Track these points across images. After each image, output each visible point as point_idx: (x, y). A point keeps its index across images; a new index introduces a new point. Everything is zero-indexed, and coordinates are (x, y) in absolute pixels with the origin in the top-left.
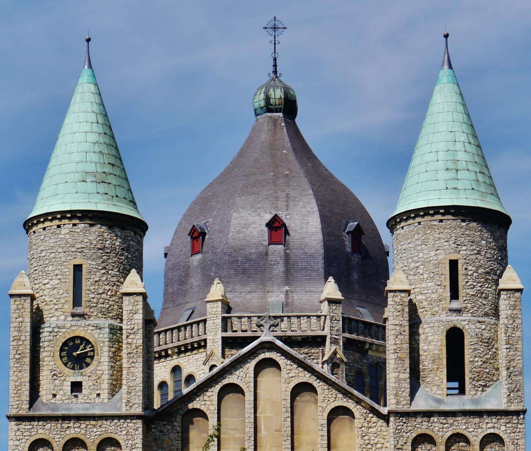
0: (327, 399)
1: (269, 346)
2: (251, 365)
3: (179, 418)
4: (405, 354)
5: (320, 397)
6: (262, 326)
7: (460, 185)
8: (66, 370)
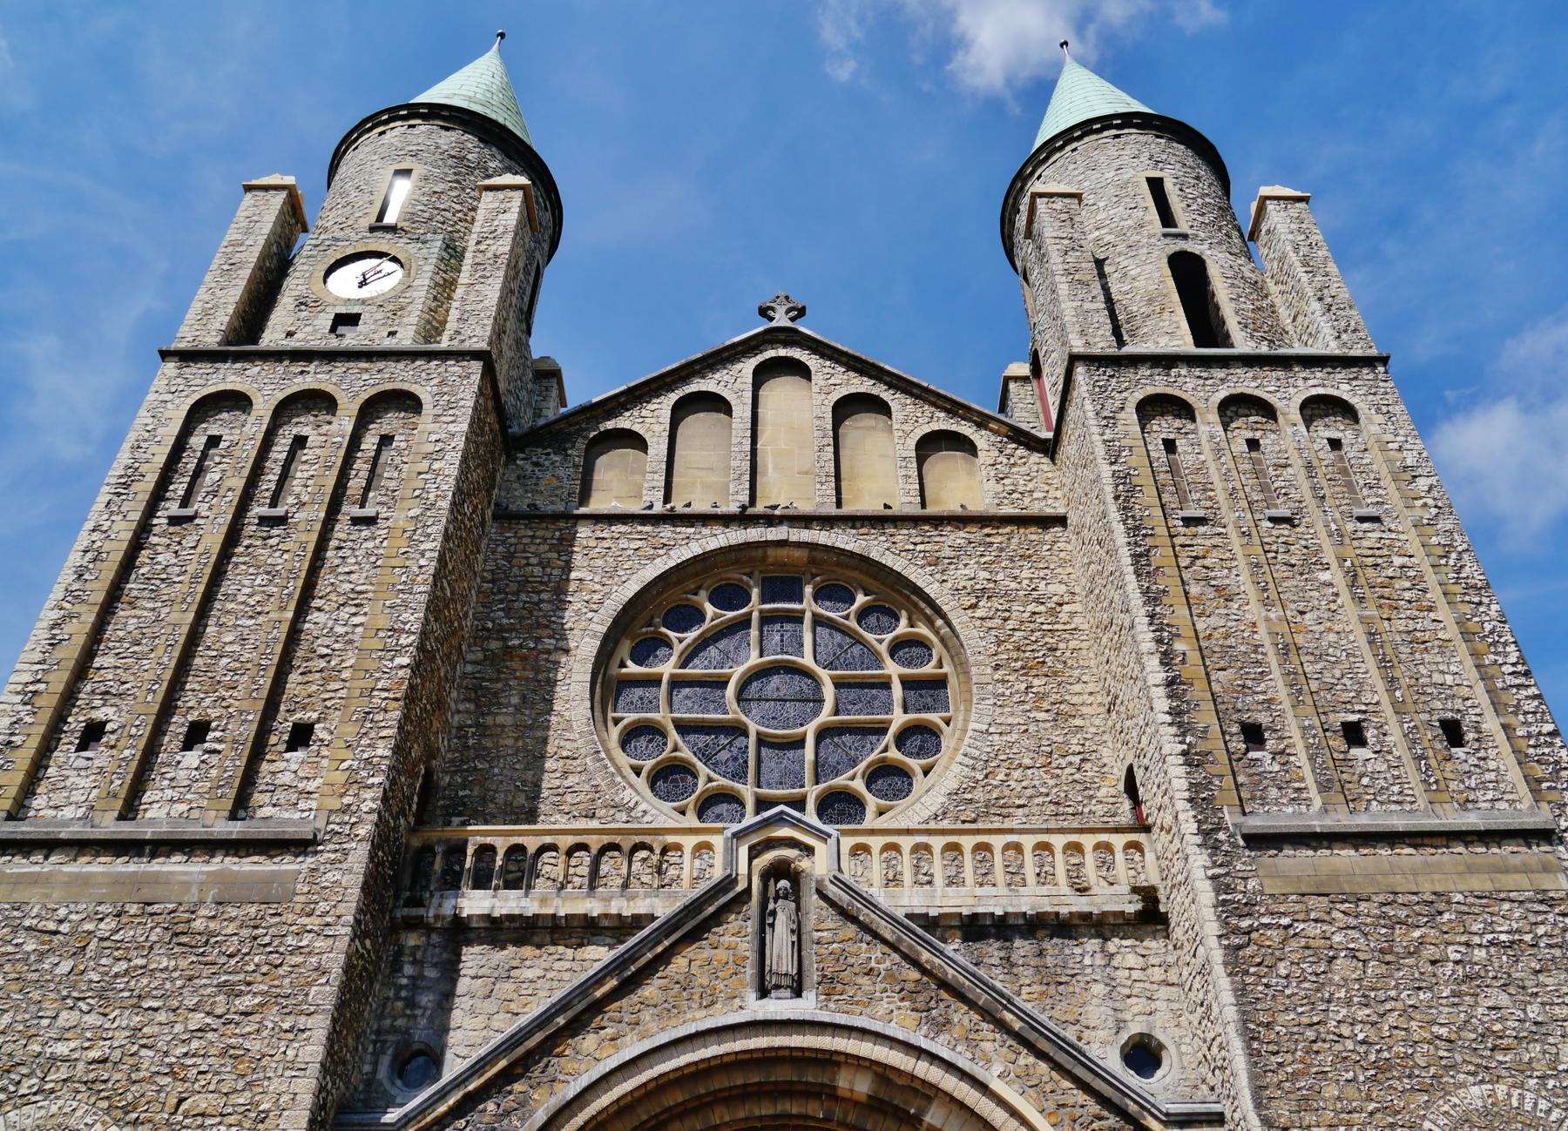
2: (748, 366)
3: (581, 444)
6: (773, 309)
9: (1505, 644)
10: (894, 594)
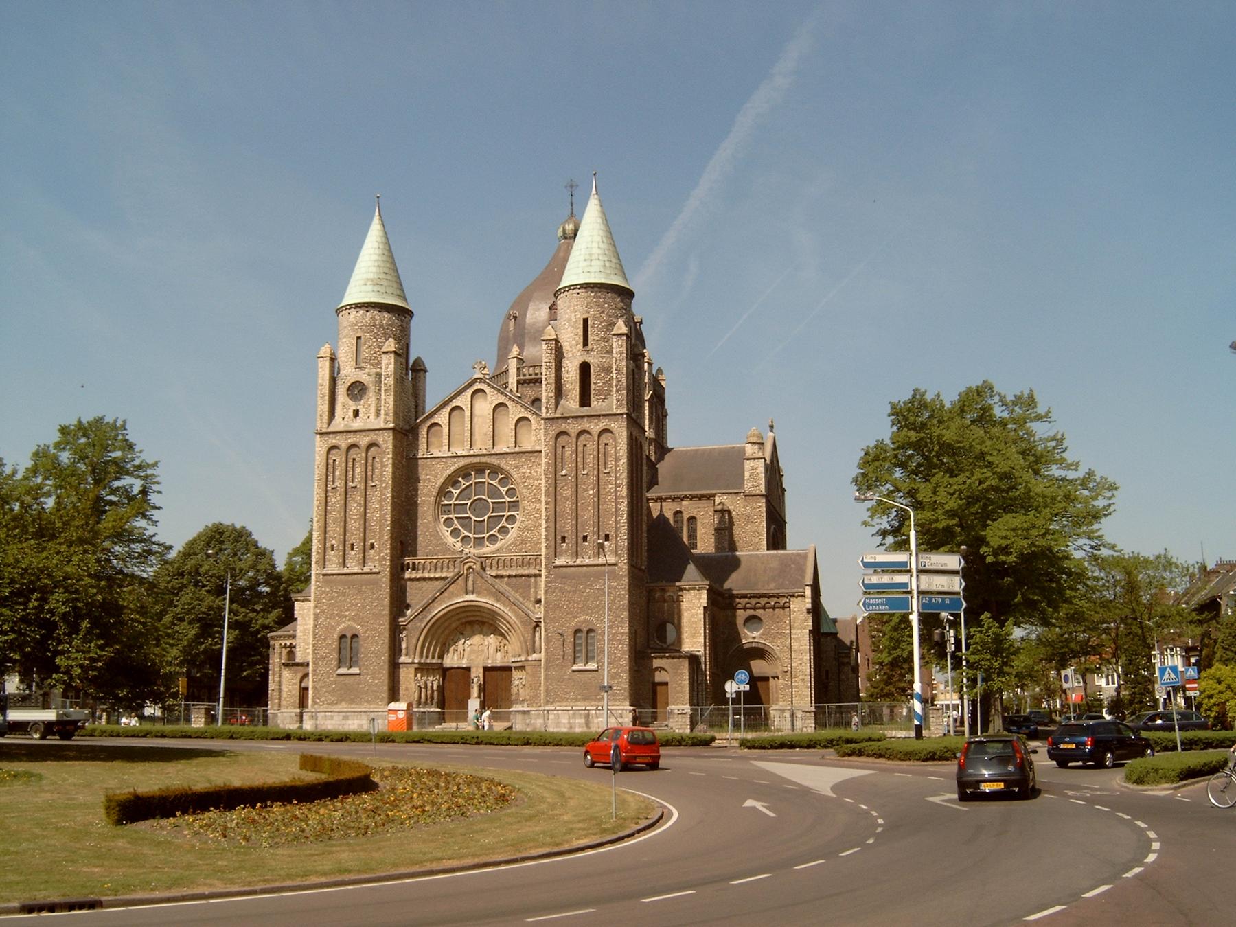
0: (515, 412)
1: (481, 380)
4: (552, 380)
7: (592, 270)
8: (351, 403)
10: (506, 479)
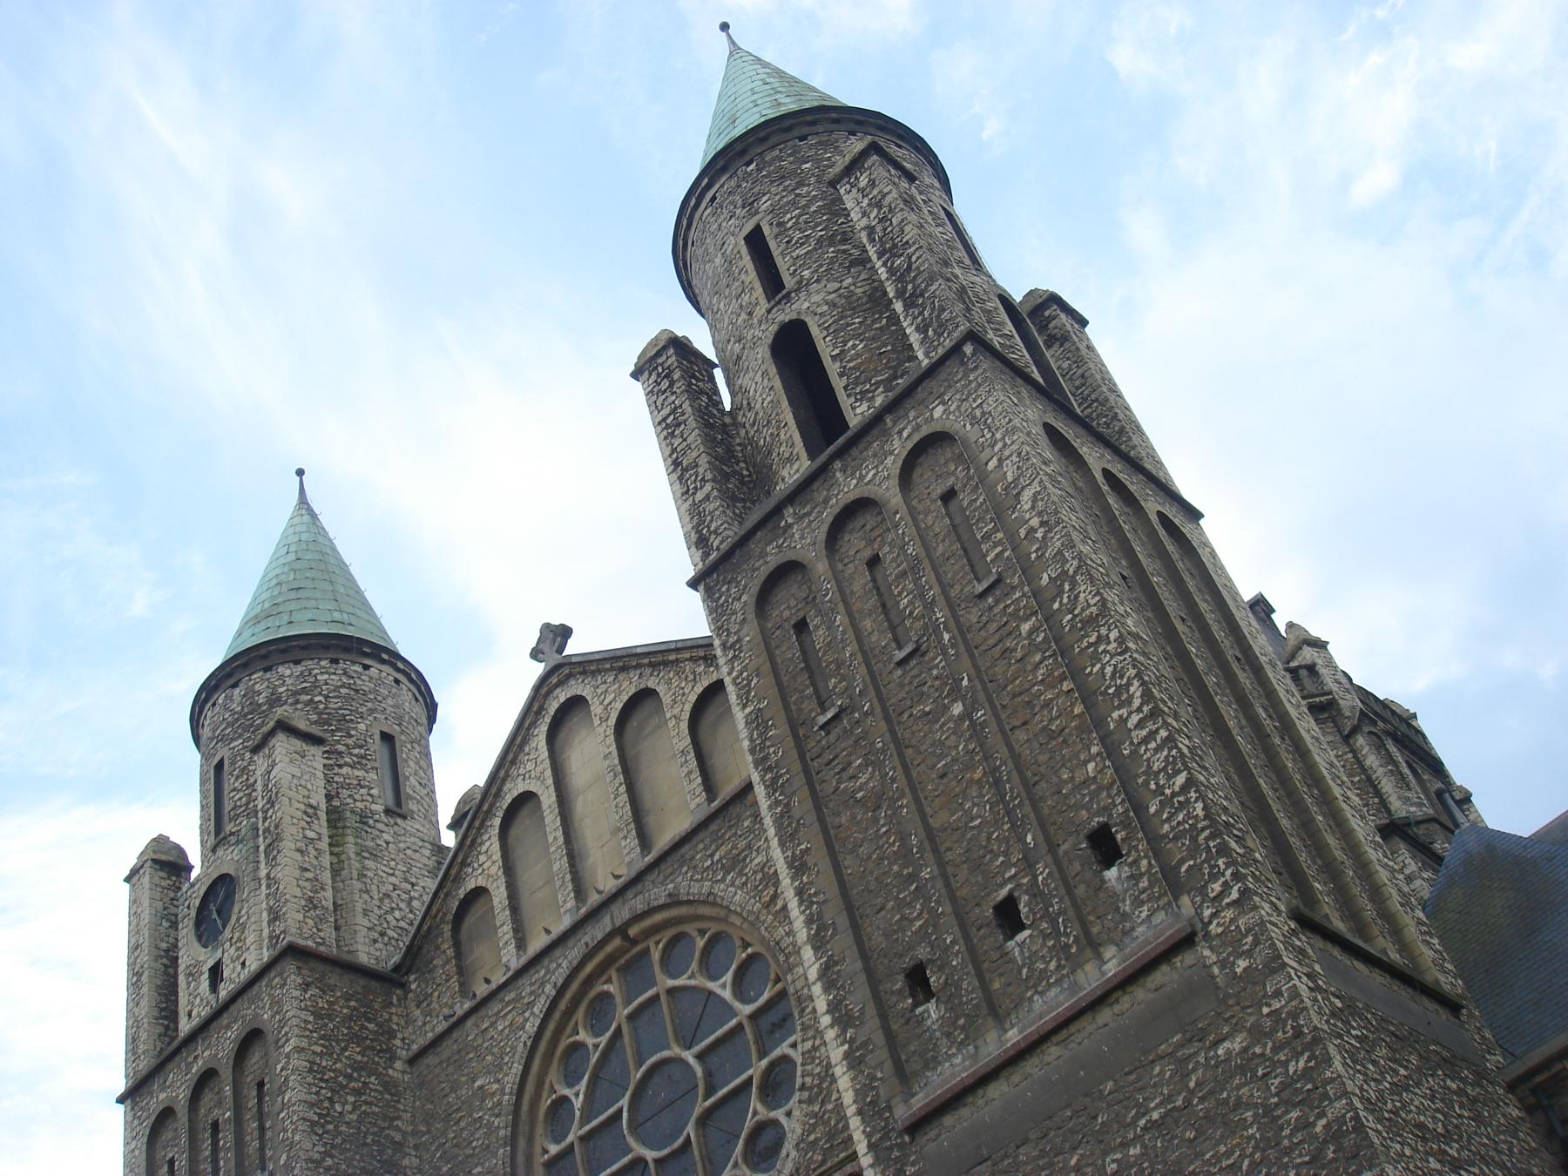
5: (666, 699)
9: (1129, 684)
